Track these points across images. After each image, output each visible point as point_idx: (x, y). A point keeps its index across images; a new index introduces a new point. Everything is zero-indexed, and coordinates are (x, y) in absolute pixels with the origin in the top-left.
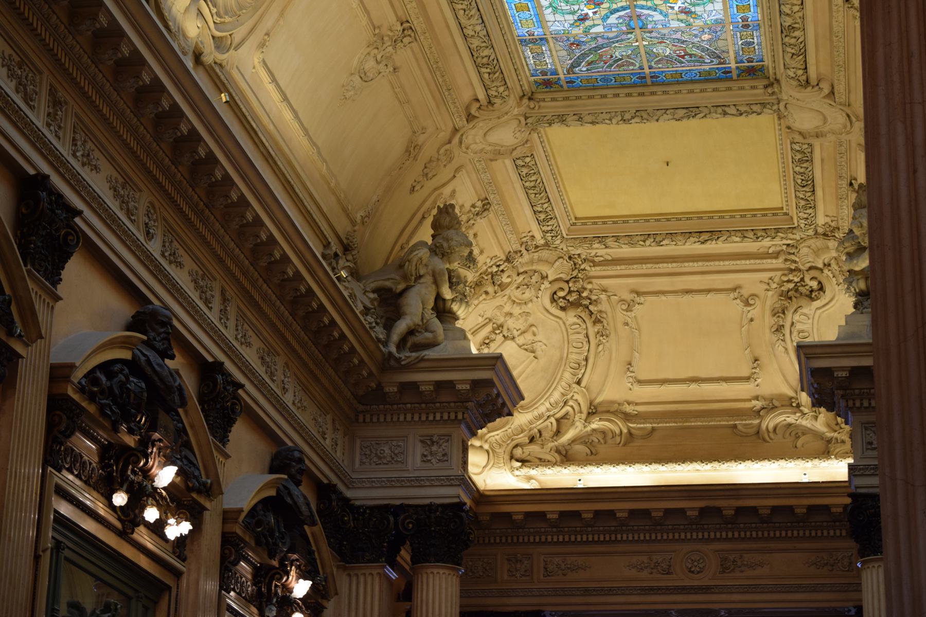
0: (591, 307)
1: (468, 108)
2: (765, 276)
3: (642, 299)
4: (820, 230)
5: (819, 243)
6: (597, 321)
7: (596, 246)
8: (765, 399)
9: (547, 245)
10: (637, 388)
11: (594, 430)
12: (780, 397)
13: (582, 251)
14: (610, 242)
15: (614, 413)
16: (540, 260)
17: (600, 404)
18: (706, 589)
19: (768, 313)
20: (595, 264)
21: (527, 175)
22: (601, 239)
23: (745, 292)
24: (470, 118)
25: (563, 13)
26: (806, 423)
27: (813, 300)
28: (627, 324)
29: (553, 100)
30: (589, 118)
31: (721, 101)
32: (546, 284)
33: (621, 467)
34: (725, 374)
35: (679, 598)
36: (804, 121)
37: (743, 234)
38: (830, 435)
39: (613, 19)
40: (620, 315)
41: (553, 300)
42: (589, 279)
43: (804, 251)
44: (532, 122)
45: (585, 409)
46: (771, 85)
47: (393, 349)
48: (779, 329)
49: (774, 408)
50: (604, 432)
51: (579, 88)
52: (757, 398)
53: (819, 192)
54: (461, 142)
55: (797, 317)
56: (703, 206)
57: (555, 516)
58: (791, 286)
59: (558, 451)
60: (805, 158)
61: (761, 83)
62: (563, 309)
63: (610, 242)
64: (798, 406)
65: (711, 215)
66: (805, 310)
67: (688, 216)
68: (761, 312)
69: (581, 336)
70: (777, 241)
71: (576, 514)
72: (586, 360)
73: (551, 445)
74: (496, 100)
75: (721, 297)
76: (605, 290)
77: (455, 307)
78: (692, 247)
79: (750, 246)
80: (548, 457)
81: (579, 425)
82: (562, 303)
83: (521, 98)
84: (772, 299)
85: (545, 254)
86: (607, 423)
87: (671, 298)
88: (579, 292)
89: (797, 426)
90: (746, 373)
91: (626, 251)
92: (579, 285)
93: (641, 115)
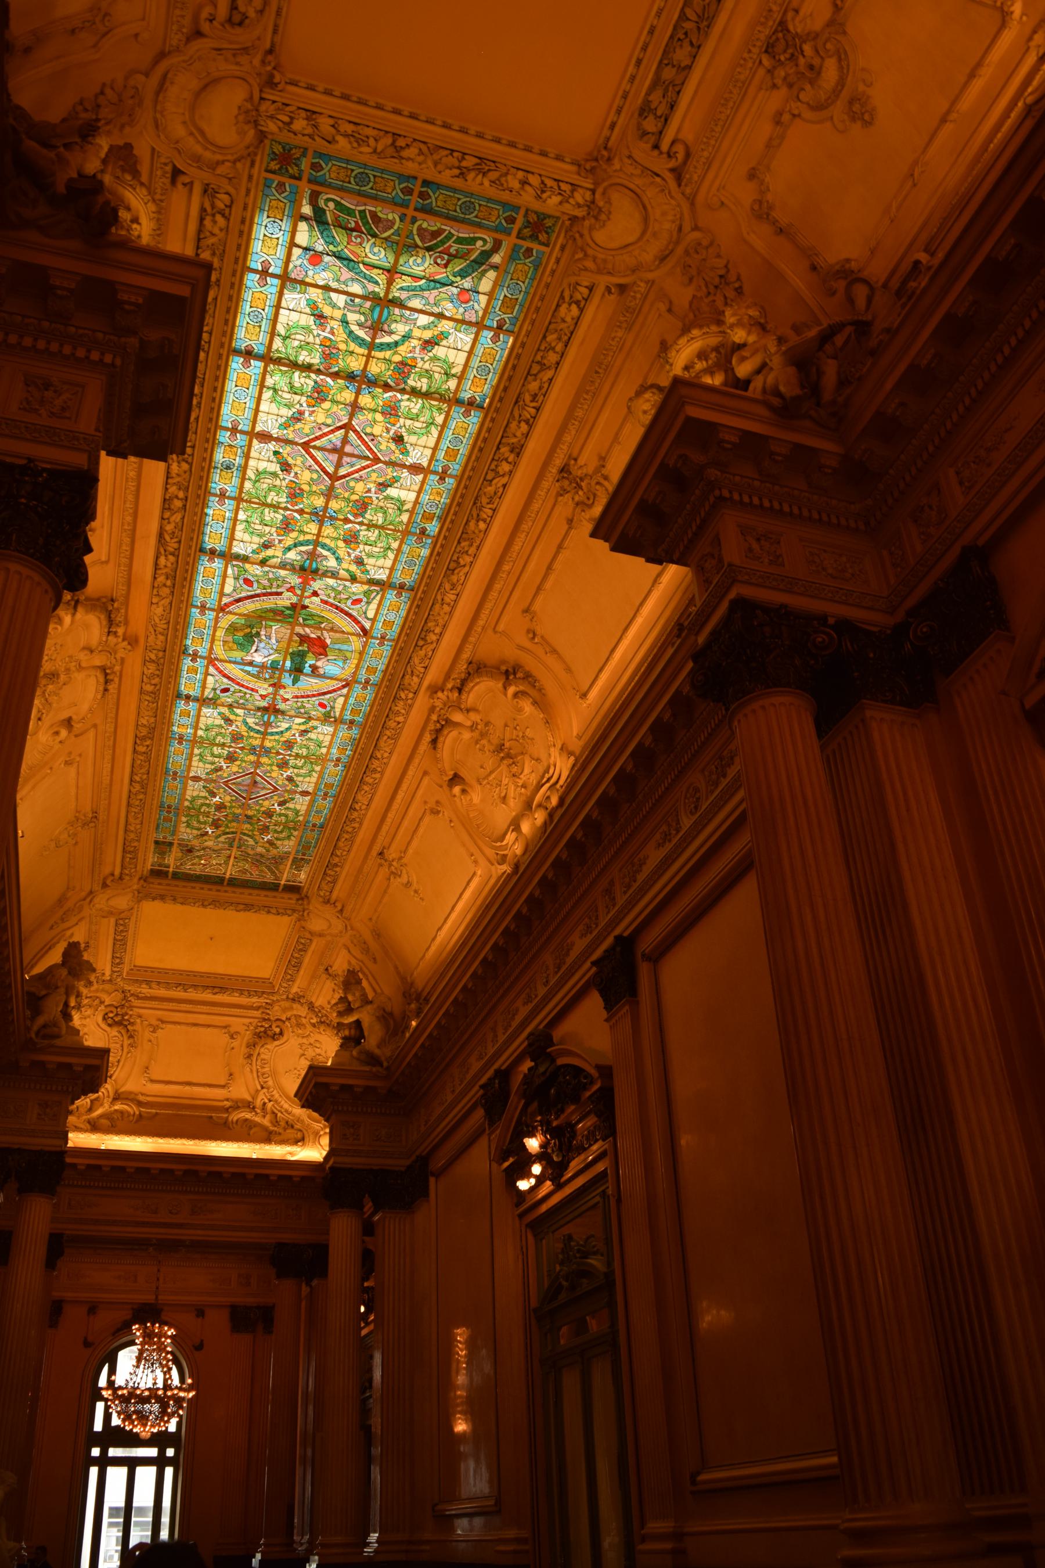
0: (129, 1027)
1: (105, 879)
2: (247, 1021)
3: (164, 1026)
4: (291, 996)
5: (287, 1004)
6: (131, 1037)
7: (144, 986)
8: (233, 1101)
9: (110, 981)
10: (150, 1085)
11: (116, 1111)
12: (243, 1101)
13: (133, 988)
14: (154, 985)
15: (132, 1100)
16: (103, 990)
17: (123, 1093)
18: (180, 1226)
19: (244, 1045)
20: (138, 998)
21: (122, 931)
22: (148, 983)
23: (232, 1030)
24: (105, 885)
25: (193, 828)
26: (257, 1119)
27: (274, 1040)
28: (150, 1041)
29: (160, 884)
30: (181, 900)
31: (267, 904)
32: (102, 1007)
33: (133, 1137)
34: (209, 1082)
35: (162, 1230)
36: (316, 924)
37: (241, 992)
38: (272, 1128)
39: (222, 839)
41: (104, 1019)
42: (131, 1007)
43: (276, 1008)
44: (143, 895)
45: (111, 1095)
46: (302, 899)
47: (33, 1036)
48: (250, 1056)
49: (238, 1107)
50: (122, 1112)
51: (178, 879)
52: (227, 1100)
53: (302, 972)
54: (91, 902)
55: (262, 1050)
56: (221, 970)
57: (83, 1167)
58: (262, 1029)
59: (89, 1122)
60: (303, 949)
61: (295, 896)
62: (110, 1025)
63: (154, 985)
64: (254, 1108)
65: (222, 976)
66: (268, 1046)
67: (208, 975)
68: (240, 1045)
69: (118, 1046)
70: (262, 1000)
71: (99, 1167)
72: (119, 1062)
73: (85, 1117)
74: (127, 878)
75: (216, 1031)
76: (140, 1016)
77: (73, 1013)
78: (208, 996)
79: (244, 1000)
80: (82, 1126)
81: (106, 1106)
82: (110, 1021)
83: (140, 879)
84: (248, 1036)
85: (107, 987)
86: (125, 1107)
87: (183, 1027)
88: (123, 1015)
89: (251, 1121)
90: (223, 1083)
91: (162, 992)
92: (123, 1011)
93: (216, 903)
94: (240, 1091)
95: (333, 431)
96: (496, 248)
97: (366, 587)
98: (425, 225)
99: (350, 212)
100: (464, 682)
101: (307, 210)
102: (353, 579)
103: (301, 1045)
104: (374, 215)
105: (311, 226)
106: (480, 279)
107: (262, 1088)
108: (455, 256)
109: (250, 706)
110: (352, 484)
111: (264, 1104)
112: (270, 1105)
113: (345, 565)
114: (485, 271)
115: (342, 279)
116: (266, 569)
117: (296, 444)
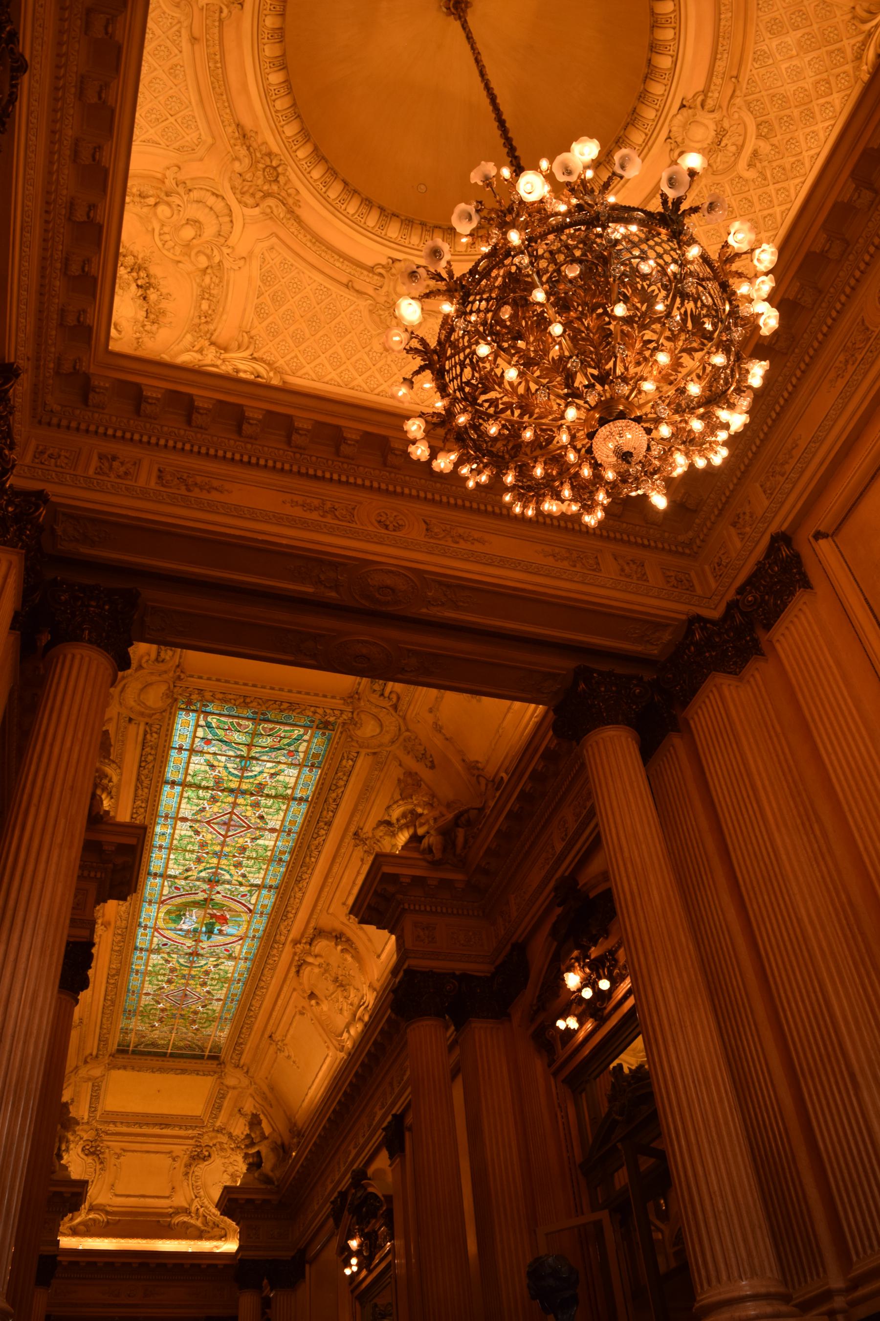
2: (185, 1147)
23: (174, 1154)
27: (205, 1161)
40: (113, 1160)
48: (187, 1174)
52: (171, 1207)
68: (180, 1165)
76: (108, 1147)
87: (139, 1154)
90: (167, 1195)
94: (179, 1200)
103: (224, 1164)
107: (196, 1197)
111: (198, 1209)
112: (201, 1210)
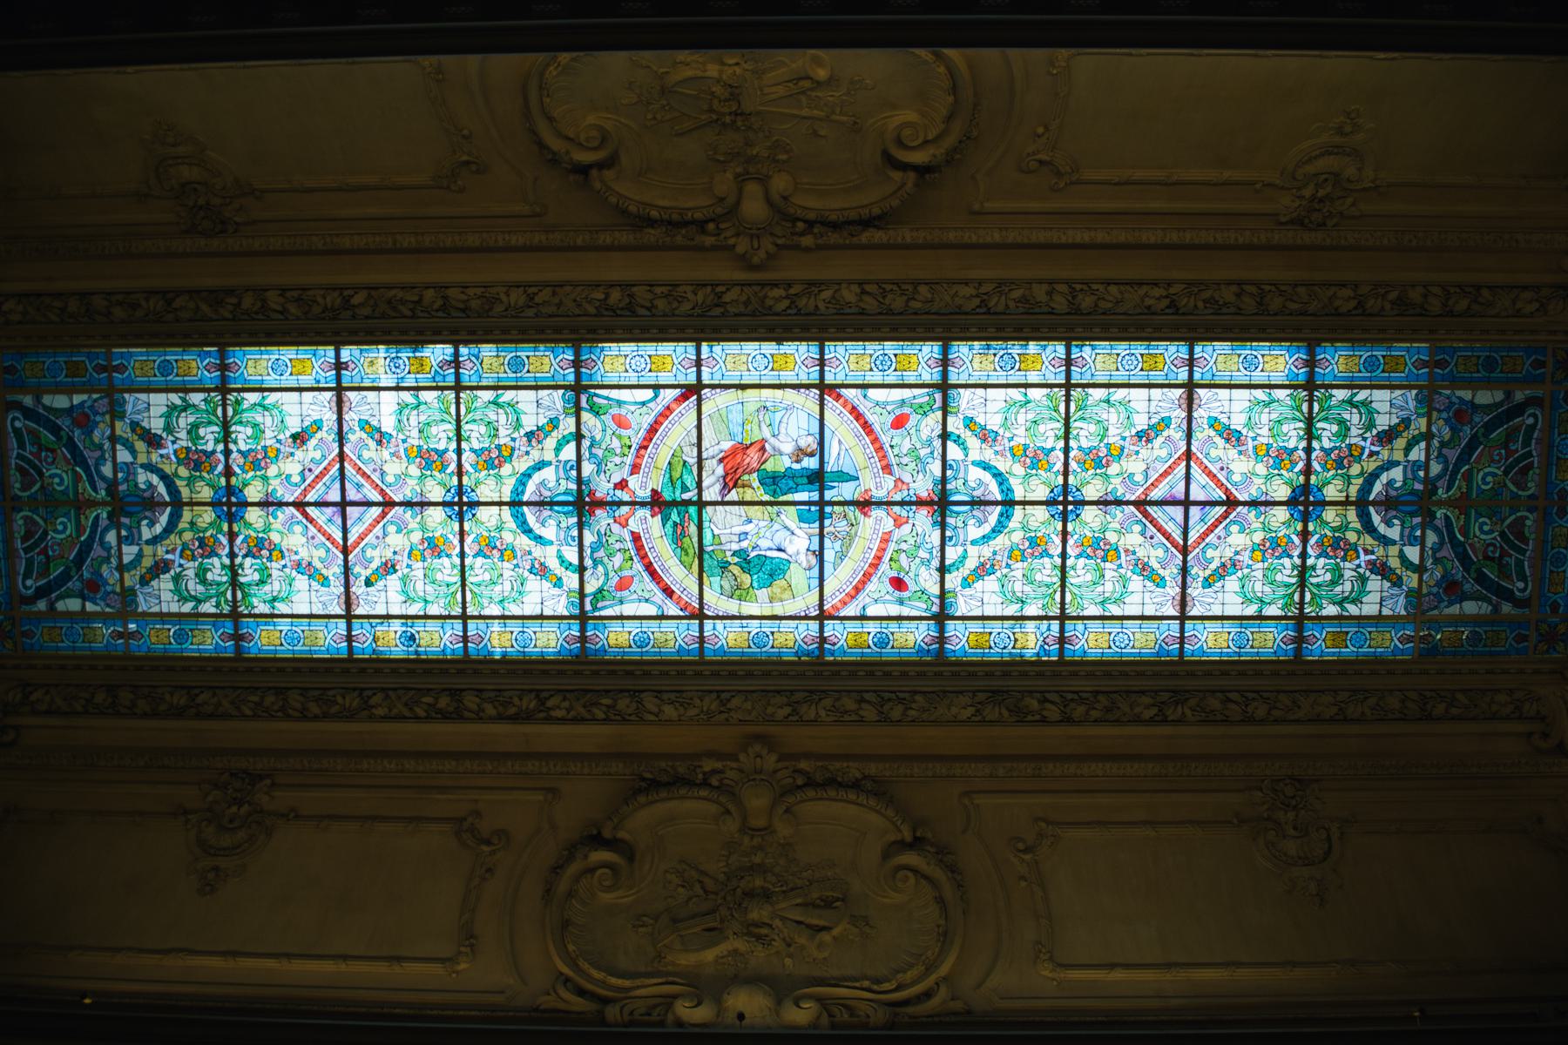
95: (1220, 485)
96: (1517, 603)
97: (936, 590)
98: (1528, 523)
99: (1526, 443)
100: (832, 782)
101: (1519, 396)
102: (943, 570)
104: (1530, 466)
105: (1501, 404)
106: (1477, 599)
108: (1500, 565)
109: (588, 469)
110: (1137, 528)
113: (973, 551)
114: (1489, 602)
115: (1445, 451)
116: (938, 443)
117: (1189, 444)
